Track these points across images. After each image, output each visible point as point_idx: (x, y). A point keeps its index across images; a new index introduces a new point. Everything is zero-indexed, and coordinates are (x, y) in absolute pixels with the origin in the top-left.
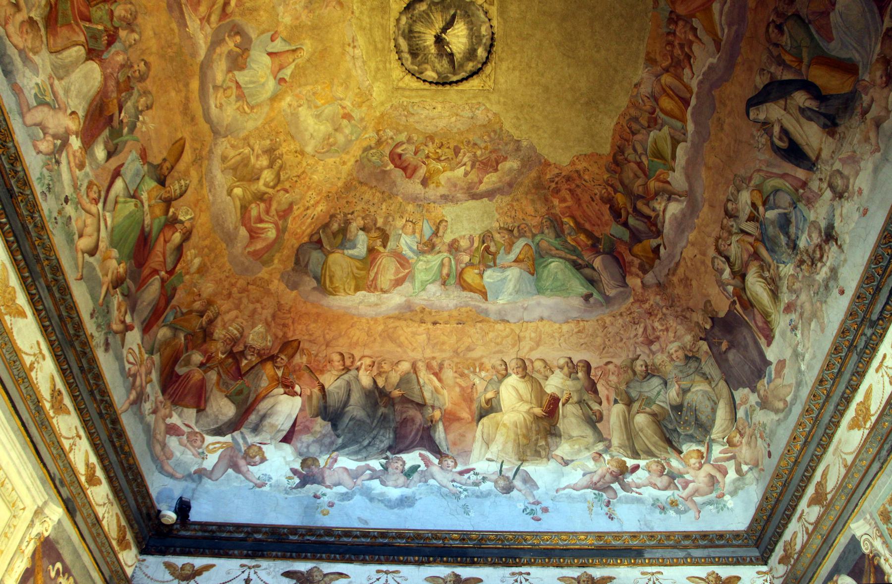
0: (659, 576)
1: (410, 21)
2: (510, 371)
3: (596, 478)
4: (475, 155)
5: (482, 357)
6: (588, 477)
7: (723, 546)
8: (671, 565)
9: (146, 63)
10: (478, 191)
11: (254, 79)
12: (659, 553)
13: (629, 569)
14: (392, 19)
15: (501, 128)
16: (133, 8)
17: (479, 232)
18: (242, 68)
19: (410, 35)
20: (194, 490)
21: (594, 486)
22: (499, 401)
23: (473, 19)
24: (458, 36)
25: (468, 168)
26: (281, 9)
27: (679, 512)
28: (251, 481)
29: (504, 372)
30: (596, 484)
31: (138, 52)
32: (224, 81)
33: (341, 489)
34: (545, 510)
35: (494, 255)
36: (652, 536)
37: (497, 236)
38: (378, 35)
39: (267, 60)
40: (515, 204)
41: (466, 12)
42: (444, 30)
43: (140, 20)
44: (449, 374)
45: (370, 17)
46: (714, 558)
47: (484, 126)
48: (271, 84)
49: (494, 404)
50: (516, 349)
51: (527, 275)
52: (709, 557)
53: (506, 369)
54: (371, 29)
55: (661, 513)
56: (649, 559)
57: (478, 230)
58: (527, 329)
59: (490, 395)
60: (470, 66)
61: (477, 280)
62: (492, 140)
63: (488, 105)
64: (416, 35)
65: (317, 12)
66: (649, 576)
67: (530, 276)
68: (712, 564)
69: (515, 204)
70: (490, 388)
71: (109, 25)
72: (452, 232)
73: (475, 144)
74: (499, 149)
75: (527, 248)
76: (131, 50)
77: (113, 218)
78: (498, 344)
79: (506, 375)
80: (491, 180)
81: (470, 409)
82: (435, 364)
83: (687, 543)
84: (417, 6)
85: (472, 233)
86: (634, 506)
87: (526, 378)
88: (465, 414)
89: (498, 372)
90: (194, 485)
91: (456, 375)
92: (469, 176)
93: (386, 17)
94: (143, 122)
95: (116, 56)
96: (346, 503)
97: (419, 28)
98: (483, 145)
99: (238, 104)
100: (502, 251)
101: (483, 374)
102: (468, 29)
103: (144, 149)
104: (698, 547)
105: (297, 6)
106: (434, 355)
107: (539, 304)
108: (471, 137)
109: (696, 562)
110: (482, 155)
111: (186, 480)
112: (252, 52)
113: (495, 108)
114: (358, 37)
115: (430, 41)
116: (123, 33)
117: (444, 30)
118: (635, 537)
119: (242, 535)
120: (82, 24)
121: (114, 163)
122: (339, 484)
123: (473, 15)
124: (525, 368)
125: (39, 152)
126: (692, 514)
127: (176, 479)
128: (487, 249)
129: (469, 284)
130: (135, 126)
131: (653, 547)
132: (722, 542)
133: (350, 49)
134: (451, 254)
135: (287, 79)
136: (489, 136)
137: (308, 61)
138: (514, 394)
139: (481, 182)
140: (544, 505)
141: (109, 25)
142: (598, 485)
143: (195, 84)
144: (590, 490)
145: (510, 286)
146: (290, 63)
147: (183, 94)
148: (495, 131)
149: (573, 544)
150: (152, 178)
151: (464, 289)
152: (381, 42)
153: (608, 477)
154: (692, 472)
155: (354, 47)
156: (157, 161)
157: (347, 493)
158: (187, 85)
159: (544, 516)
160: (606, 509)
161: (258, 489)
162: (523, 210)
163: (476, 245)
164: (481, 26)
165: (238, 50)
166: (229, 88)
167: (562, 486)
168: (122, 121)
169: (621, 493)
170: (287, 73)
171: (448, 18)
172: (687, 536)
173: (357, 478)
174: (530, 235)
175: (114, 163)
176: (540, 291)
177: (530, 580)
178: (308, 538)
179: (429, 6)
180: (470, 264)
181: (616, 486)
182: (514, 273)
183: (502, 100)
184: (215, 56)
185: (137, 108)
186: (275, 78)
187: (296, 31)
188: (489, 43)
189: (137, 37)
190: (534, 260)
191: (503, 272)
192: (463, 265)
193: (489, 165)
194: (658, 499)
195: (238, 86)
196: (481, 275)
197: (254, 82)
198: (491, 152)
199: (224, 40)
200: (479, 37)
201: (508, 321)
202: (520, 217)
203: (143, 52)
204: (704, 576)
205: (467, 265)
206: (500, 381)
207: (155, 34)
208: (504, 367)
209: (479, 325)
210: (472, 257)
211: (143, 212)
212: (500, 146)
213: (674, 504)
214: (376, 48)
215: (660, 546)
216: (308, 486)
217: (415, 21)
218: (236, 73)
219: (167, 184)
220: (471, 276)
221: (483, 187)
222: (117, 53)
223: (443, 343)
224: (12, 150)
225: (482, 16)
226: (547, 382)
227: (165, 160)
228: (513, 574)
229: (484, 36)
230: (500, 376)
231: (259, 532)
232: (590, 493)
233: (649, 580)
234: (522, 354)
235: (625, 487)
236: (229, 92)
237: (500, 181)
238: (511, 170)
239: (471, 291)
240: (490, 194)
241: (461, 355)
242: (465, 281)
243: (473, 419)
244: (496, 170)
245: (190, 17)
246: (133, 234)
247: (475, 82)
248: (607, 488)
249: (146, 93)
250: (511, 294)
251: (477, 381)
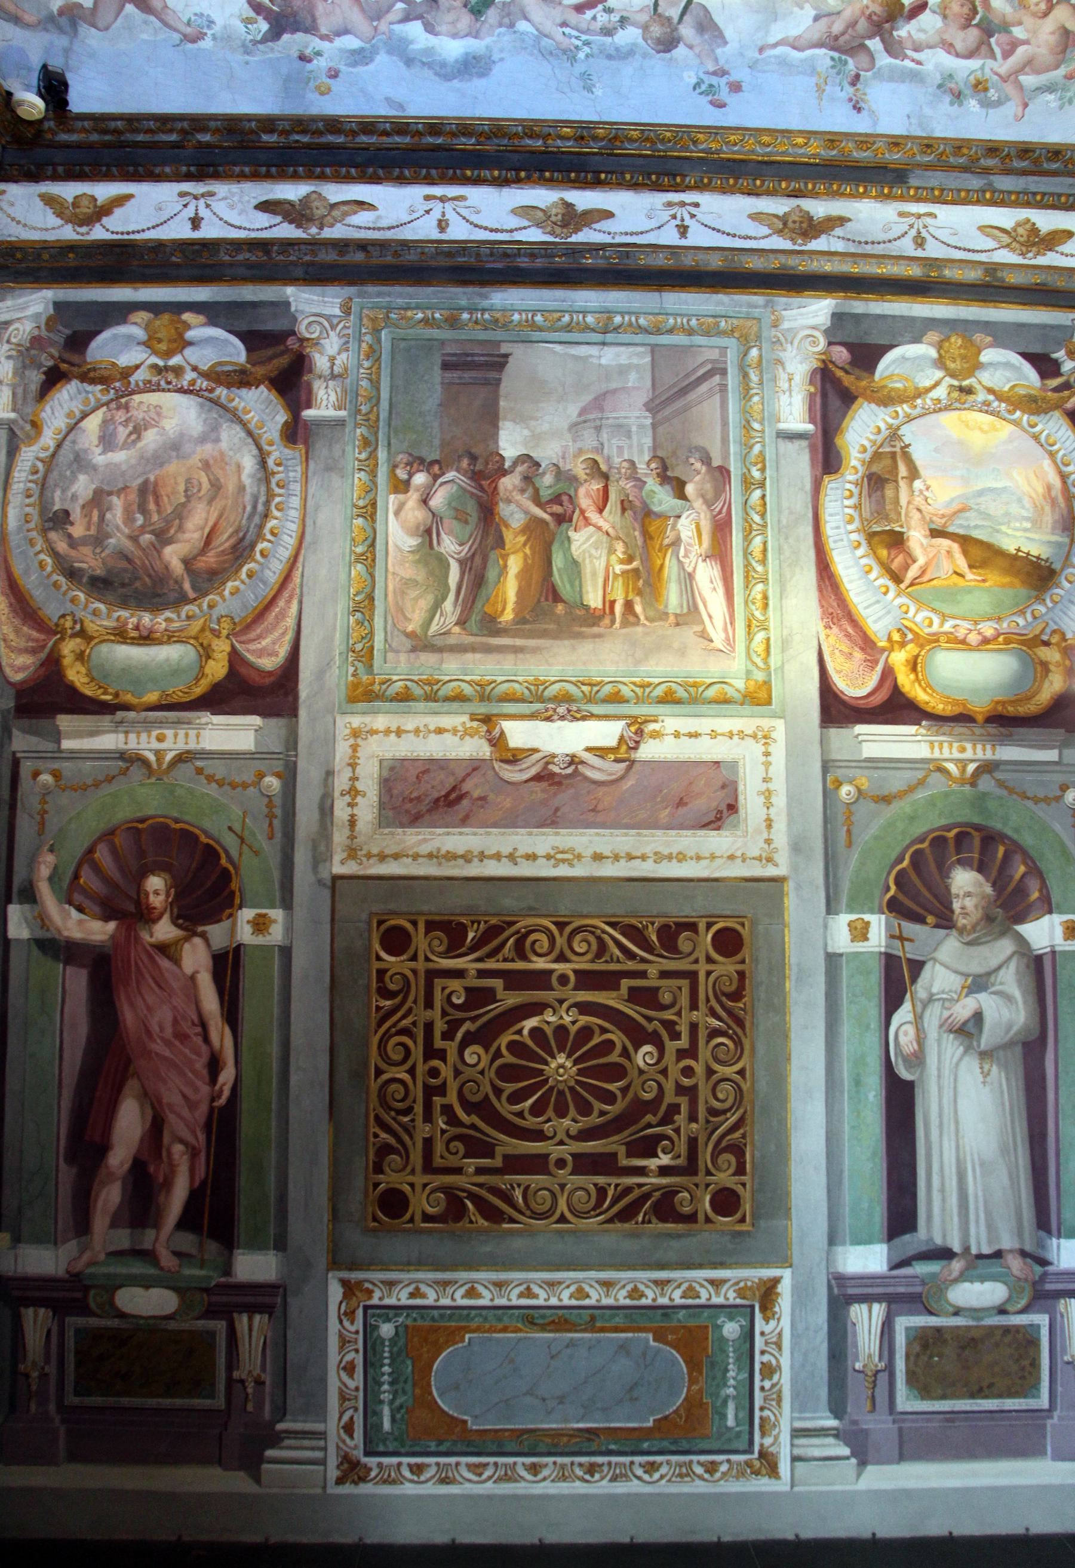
0: (929, 220)
3: (837, 27)
6: (824, 22)
7: (1055, 173)
8: (954, 202)
12: (935, 179)
13: (878, 205)
20: (67, 52)
21: (832, 42)
27: (986, 104)
28: (175, 30)
30: (836, 38)
33: (350, 42)
34: (736, 87)
36: (928, 146)
46: (1035, 194)
52: (1026, 193)
55: (952, 104)
56: (917, 188)
66: (912, 220)
68: (1028, 205)
83: (990, 162)
86: (903, 88)
90: (62, 41)
104: (1008, 172)
109: (1000, 200)
111: (46, 30)
118: (896, 144)
119: (173, 137)
122: (346, 32)
126: (1011, 108)
127: (27, 26)
131: (928, 167)
132: (1055, 166)
140: (734, 77)
142: (842, 40)
144: (823, 51)
149: (784, 153)
153: (862, 25)
154: (1028, 21)
157: (362, 49)
159: (731, 99)
160: (851, 90)
161: (190, 46)
167: (772, 40)
169: (884, 60)
172: (993, 149)
173: (379, 19)
177: (699, 216)
178: (297, 137)
181: (875, 44)
194: (951, 76)
204: (1008, 225)
213: (980, 86)
215: (941, 165)
216: (286, 37)
228: (670, 204)
231: (204, 129)
232: (823, 56)
233: (911, 226)
235: (893, 48)
248: (857, 48)
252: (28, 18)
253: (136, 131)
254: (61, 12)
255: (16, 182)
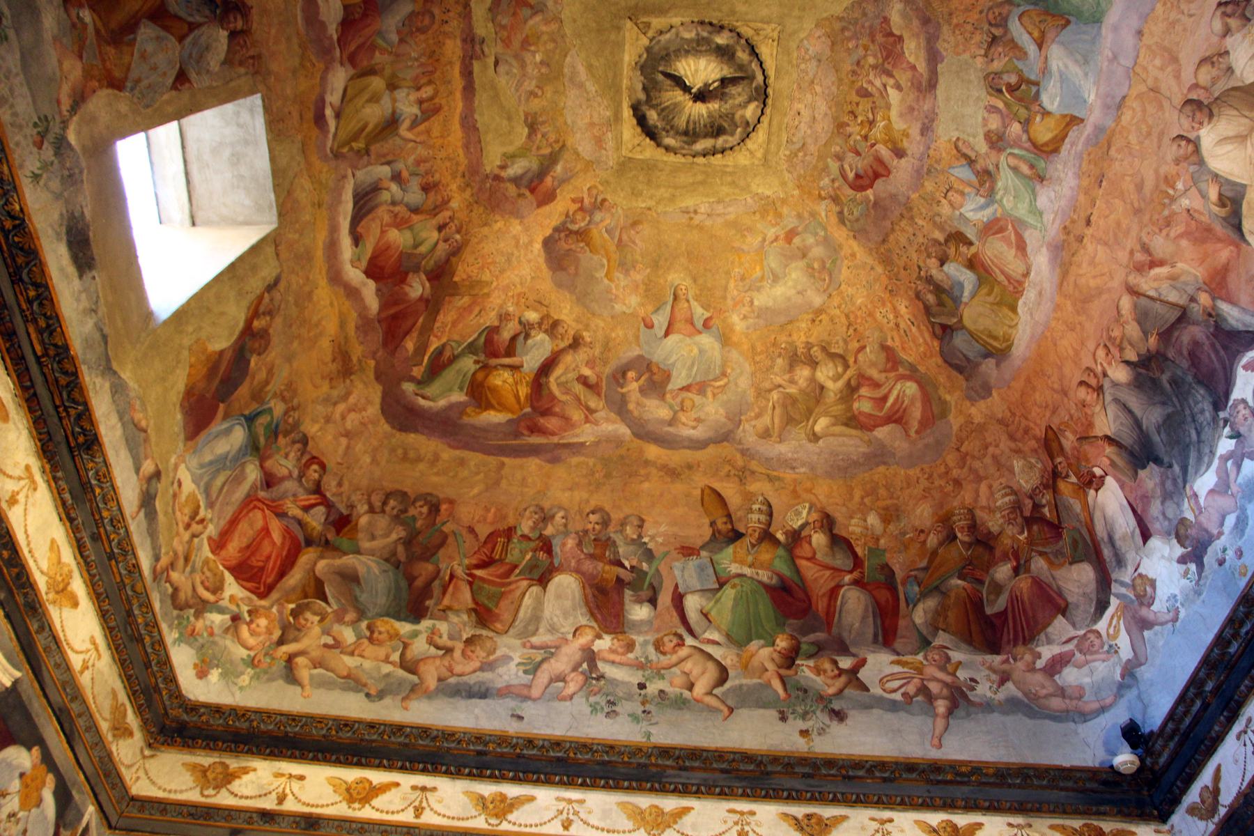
1: (672, 133)
2: (1192, 136)
4: (874, 67)
5: (1156, 172)
9: (593, 512)
10: (926, 76)
11: (689, 363)
14: (665, 158)
15: (840, 19)
16: (532, 509)
17: (983, 94)
18: (668, 377)
19: (690, 134)
22: (1228, 182)
23: (672, 49)
24: (696, 71)
25: (891, 81)
26: (619, 307)
29: (1191, 148)
31: (578, 517)
32: (671, 407)
35: (1023, 80)
37: (997, 65)
38: (684, 179)
39: (673, 338)
40: (955, 21)
41: (662, 58)
42: (686, 89)
43: (546, 504)
44: (1160, 245)
45: (658, 187)
47: (833, 44)
48: (706, 340)
49: (1229, 194)
50: (1166, 104)
51: (1066, 34)
53: (1189, 141)
54: (676, 188)
57: (979, 92)
58: (1145, 69)
59: (1213, 194)
60: (742, 55)
61: (1050, 122)
62: (855, 36)
63: (802, 35)
64: (691, 127)
65: (638, 257)
67: (1069, 28)
69: (955, 21)
70: (1203, 186)
71: (533, 545)
72: (974, 137)
73: (858, 63)
74: (871, 27)
75: (1025, 19)
76: (569, 526)
77: (718, 629)
78: (1149, 134)
79: (1196, 144)
80: (913, 50)
81: (1219, 240)
82: (1140, 257)
84: (651, 122)
85: (982, 104)
87: (1215, 111)
88: (1224, 254)
89: (1186, 158)
91: (1164, 232)
92: (902, 83)
93: (661, 165)
94: (652, 538)
95: (566, 547)
96: (1247, 531)
97: (681, 122)
98: (861, 52)
99: (709, 394)
100: (1020, 65)
101: (1180, 186)
102: (686, 57)
103: (683, 548)
105: (622, 284)
106: (1128, 250)
107: (1115, 29)
108: (847, 66)
110: (875, 56)
112: (655, 359)
113: (809, 24)
114: (683, 205)
115: (701, 109)
116: (549, 531)
117: (686, 89)
120: (513, 578)
121: (665, 599)
122: (1223, 518)
123: (666, 49)
124: (1198, 104)
125: (571, 697)
128: (1012, 89)
129: (1055, 137)
130: (650, 551)
133: (698, 219)
134: (1004, 149)
135: (707, 315)
136: (849, 39)
137: (695, 280)
138: (1230, 147)
139: (913, 68)
141: (533, 545)
143: (653, 451)
145: (1075, 70)
146: (690, 307)
147: (654, 471)
148: (843, 29)
150: (721, 549)
151: (1056, 150)
152: (695, 175)
155: (696, 212)
156: (707, 532)
158: (647, 463)
161: (1178, 624)
162: (967, 10)
163: (1001, 105)
164: (682, 39)
165: (643, 378)
166: (682, 402)
168: (632, 567)
170: (700, 313)
171: (669, 82)
174: (1007, 7)
175: (665, 599)
176: (1096, 19)
178: (1244, 630)
179: (653, 107)
180: (1026, 124)
182: (1057, 57)
183: (796, 13)
184: (636, 413)
185: (633, 540)
186: (700, 333)
187: (650, 291)
188: (709, 28)
189: (561, 514)
190: (1047, 13)
191: (1050, 72)
192: (1025, 137)
193: (891, 48)
195: (687, 388)
196: (1046, 113)
197: (693, 364)
198: (873, 41)
199: (623, 395)
200: (700, 41)
201: (1124, 97)
202: (977, 16)
203: (580, 511)
205: (1026, 131)
206: (1201, 162)
207: (570, 489)
208: (1183, 143)
209: (1113, 152)
210: (1015, 117)
211: (751, 578)
212: (867, 24)
214: (703, 183)
216: (1206, 560)
217: (672, 127)
218: (670, 387)
219: (742, 530)
220: (1044, 131)
221: (922, 67)
222: (564, 545)
223: (1118, 224)
224: (521, 741)
225: (668, 36)
226: (1238, 72)
227: (713, 524)
229: (698, 34)
230: (1194, 159)
231: (1202, 683)
234: (1178, 100)
236: (688, 404)
237: (918, 36)
238: (904, 15)
239: (1063, 139)
240: (934, 58)
241: (1143, 205)
242: (1046, 144)
243: (1237, 246)
244: (900, 38)
245: (577, 436)
246: (761, 607)
247: (765, 51)
249: (623, 524)
250: (1086, 75)
251: (1185, 202)
252: (1108, 701)
253: (1181, 720)
254: (1123, 676)
255: (1173, 812)
